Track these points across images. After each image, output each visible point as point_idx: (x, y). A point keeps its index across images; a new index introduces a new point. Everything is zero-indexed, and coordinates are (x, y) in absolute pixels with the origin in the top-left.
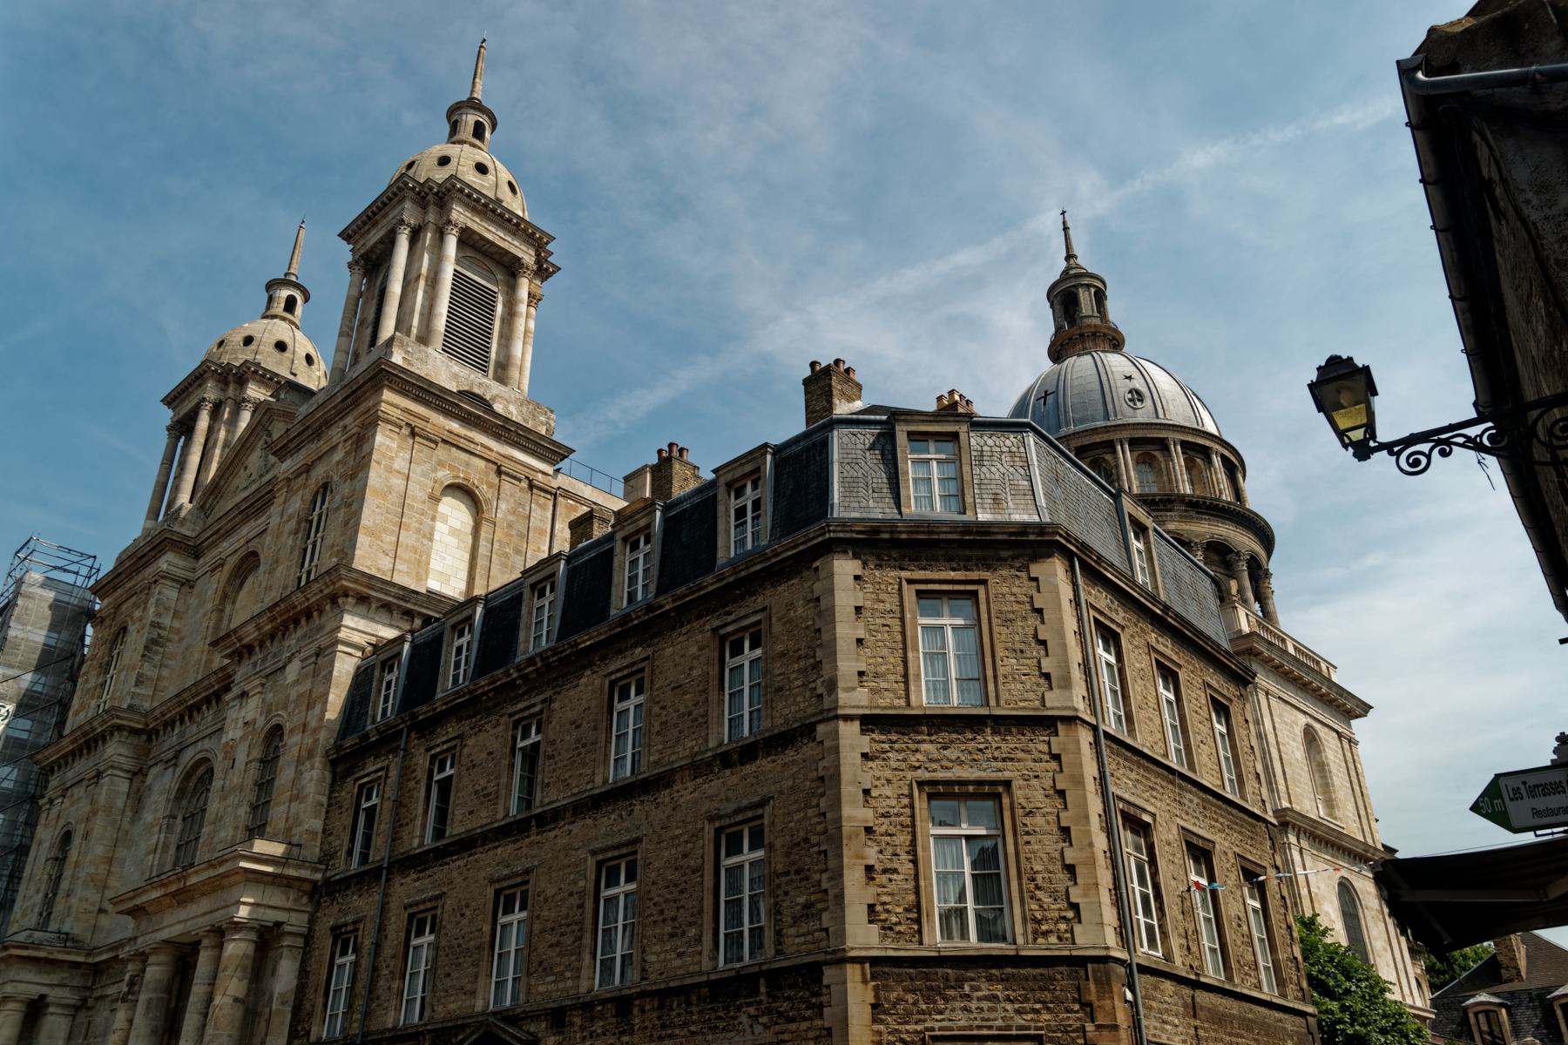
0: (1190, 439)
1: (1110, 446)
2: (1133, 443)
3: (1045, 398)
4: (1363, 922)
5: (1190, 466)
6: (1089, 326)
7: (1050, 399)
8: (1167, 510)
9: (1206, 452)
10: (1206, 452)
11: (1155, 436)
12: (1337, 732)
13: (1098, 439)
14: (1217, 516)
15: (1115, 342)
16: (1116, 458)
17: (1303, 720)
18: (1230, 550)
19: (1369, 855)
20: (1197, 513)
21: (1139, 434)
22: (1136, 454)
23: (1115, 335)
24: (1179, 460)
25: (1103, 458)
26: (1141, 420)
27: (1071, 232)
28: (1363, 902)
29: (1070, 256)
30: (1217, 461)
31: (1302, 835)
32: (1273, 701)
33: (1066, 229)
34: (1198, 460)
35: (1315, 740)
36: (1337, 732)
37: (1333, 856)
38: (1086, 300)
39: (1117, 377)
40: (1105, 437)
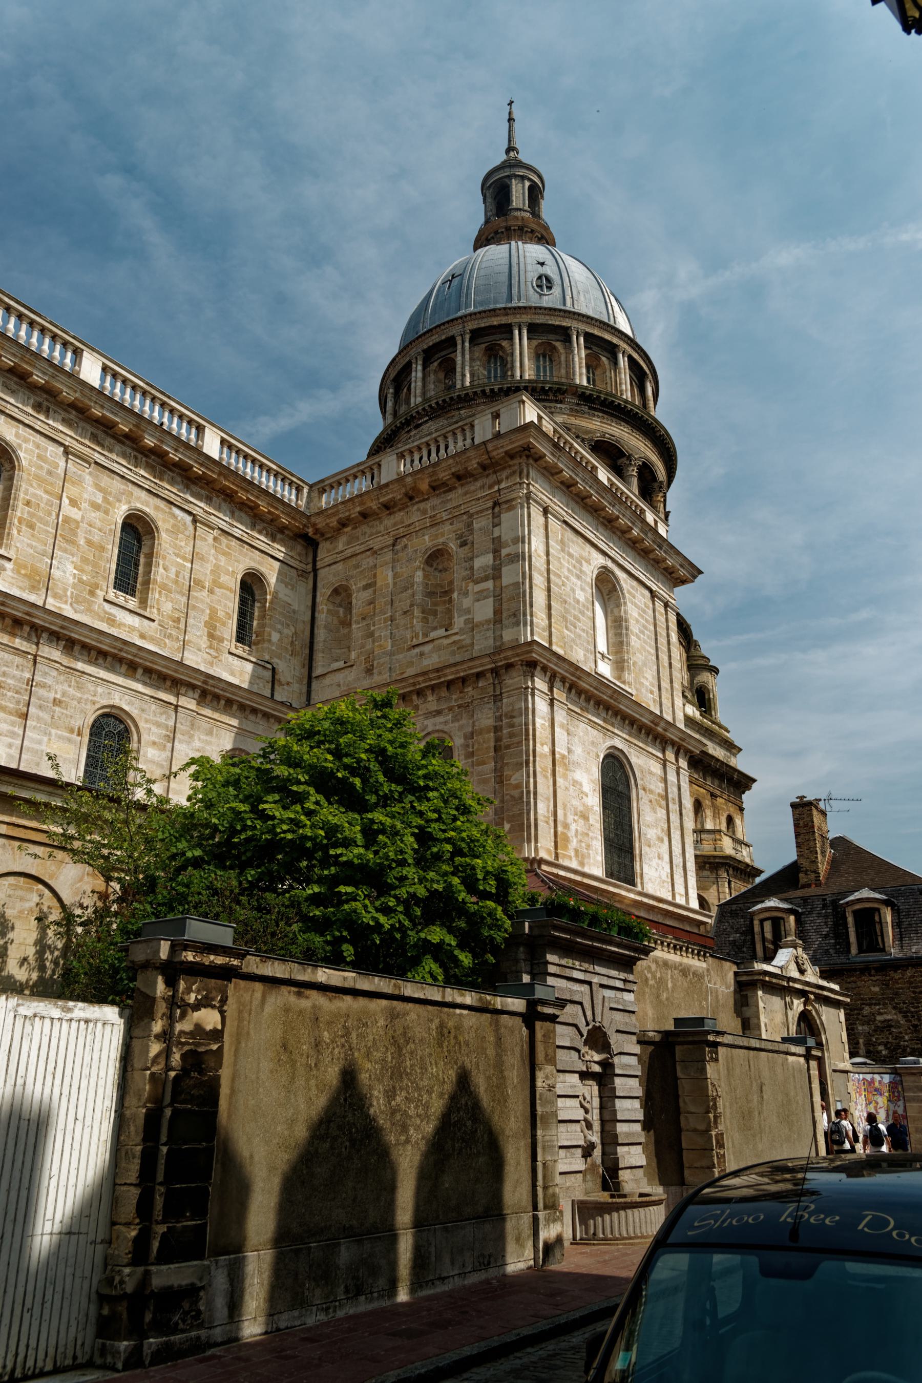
0: (596, 332)
1: (507, 330)
2: (534, 329)
3: (451, 281)
4: (634, 804)
6: (516, 218)
7: (456, 281)
8: (557, 402)
9: (612, 351)
10: (612, 351)
11: (557, 323)
12: (651, 591)
13: (495, 321)
14: (612, 415)
15: (544, 238)
16: (512, 345)
17: (599, 560)
19: (659, 729)
20: (590, 408)
21: (540, 319)
22: (535, 343)
23: (545, 234)
24: (580, 354)
25: (500, 345)
26: (545, 305)
27: (517, 125)
28: (639, 782)
29: (510, 149)
30: (623, 362)
31: (558, 683)
32: (554, 523)
33: (511, 119)
34: (604, 359)
35: (616, 590)
36: (651, 591)
37: (605, 720)
38: (519, 195)
39: (529, 261)
40: (504, 320)
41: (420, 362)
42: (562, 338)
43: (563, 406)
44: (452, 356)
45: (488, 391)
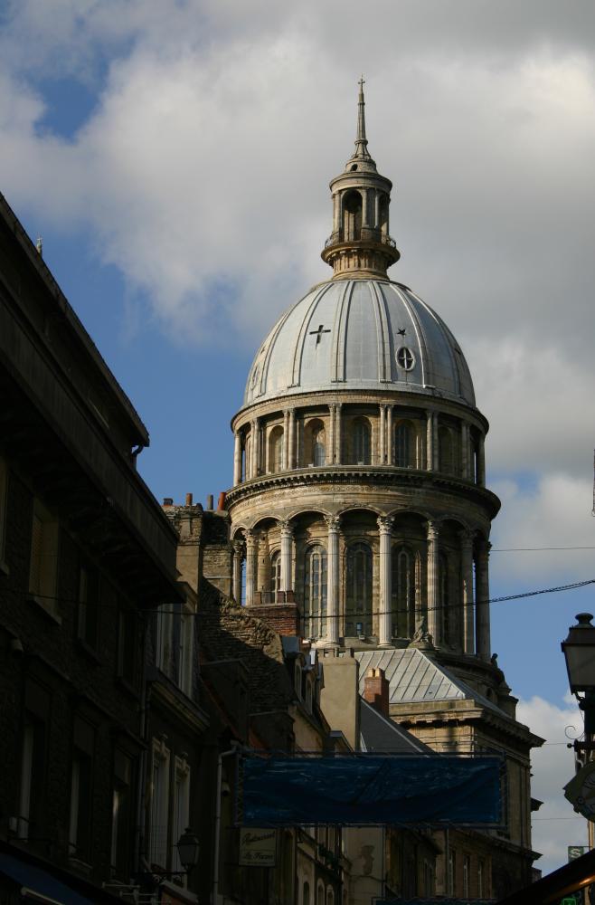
0: (448, 411)
5: (441, 433)
10: (458, 423)
18: (462, 527)
22: (398, 419)
30: (465, 430)
33: (362, 104)
34: (450, 430)
40: (372, 399)
41: (291, 418)
43: (420, 490)
44: (324, 419)
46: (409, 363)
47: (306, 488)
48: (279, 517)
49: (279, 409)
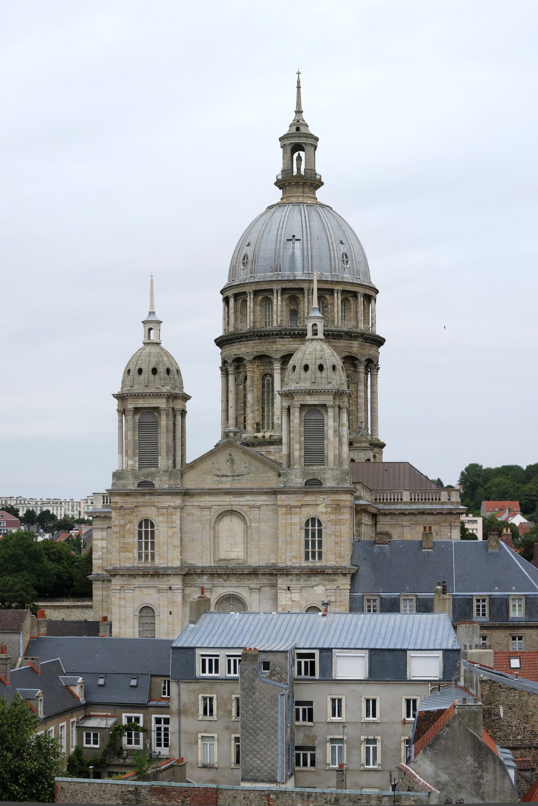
8: (354, 340)
25: (325, 297)
29: (299, 112)
33: (299, 87)
40: (330, 287)
42: (352, 295)
45: (326, 334)
46: (347, 262)
47: (291, 339)
48: (273, 355)
49: (270, 288)
